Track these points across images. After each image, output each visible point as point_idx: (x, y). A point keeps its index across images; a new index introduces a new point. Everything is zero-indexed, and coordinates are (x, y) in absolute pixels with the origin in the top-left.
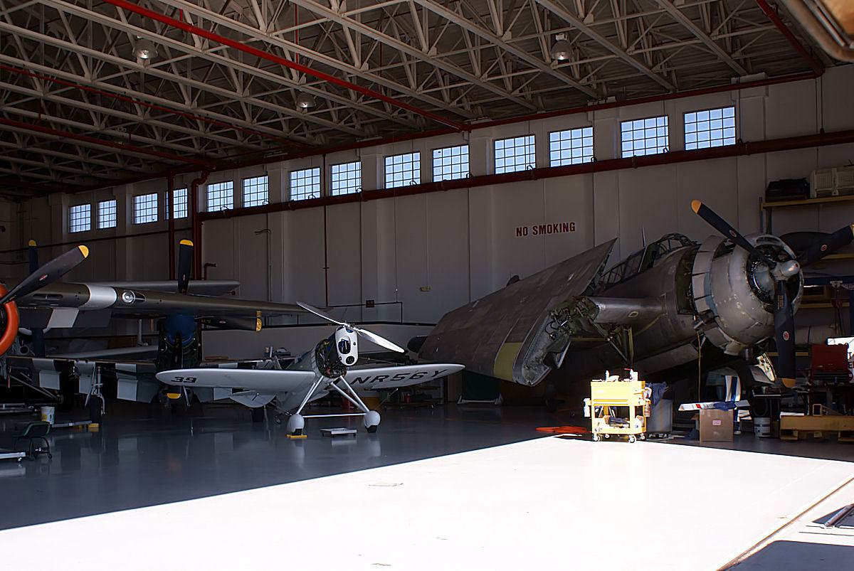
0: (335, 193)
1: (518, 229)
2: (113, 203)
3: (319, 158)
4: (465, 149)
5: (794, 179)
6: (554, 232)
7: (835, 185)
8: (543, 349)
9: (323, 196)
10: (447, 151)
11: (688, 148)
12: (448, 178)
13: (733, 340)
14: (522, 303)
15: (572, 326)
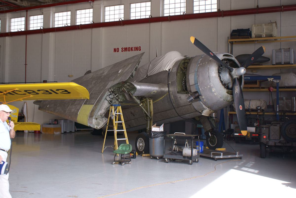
0: (31, 29)
1: (114, 49)
3: (24, 13)
4: (91, 10)
5: (244, 29)
6: (131, 51)
7: (263, 32)
10: (83, 11)
11: (195, 12)
13: (208, 108)
14: (94, 84)
15: (120, 97)
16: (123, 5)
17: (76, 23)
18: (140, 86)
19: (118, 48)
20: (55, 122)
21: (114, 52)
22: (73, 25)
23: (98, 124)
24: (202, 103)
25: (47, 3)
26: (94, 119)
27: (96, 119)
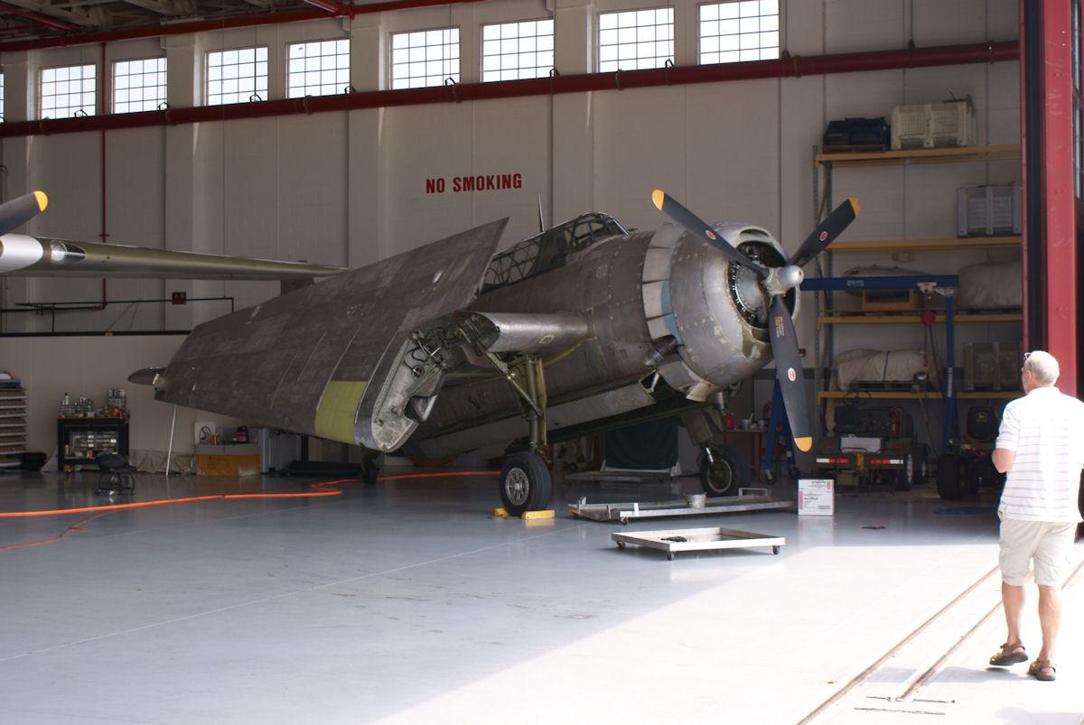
1: (428, 181)
3: (93, 49)
4: (344, 45)
6: (488, 188)
7: (928, 131)
8: (402, 392)
10: (313, 48)
12: (315, 92)
13: (702, 380)
16: (457, 30)
18: (509, 323)
19: (443, 180)
20: (238, 436)
21: (428, 192)
22: (279, 97)
23: (388, 438)
24: (686, 367)
25: (179, 17)
26: (375, 422)
27: (382, 422)
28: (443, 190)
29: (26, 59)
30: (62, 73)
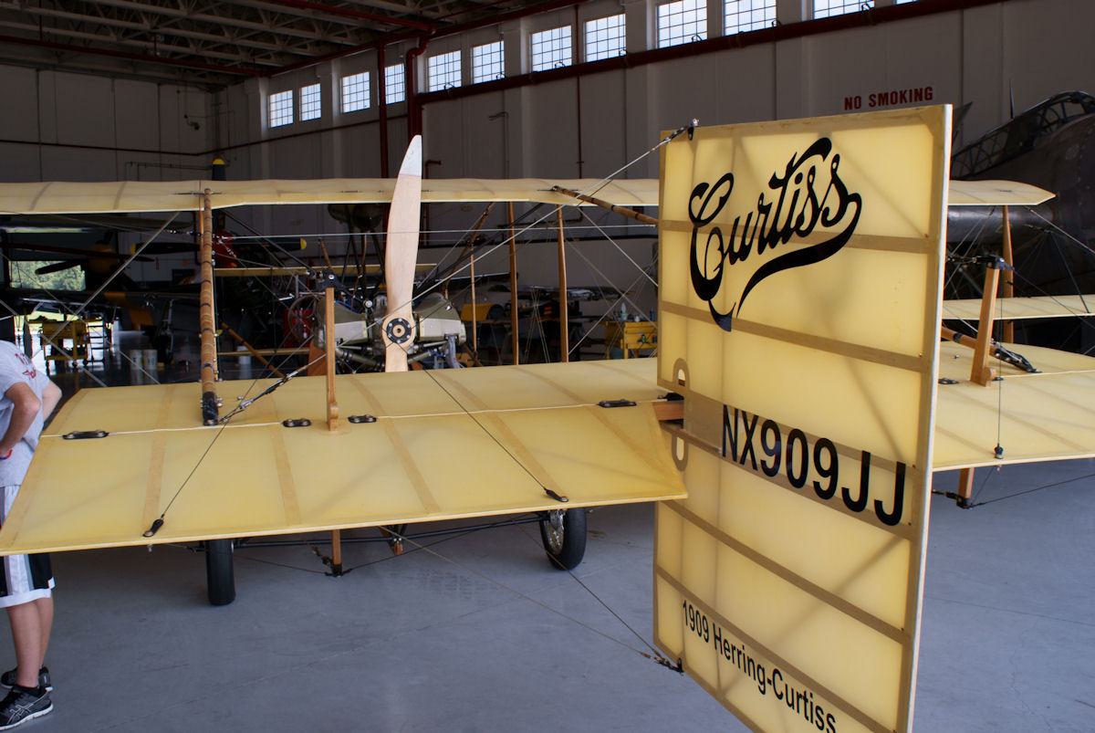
0: (591, 59)
1: (846, 99)
2: (318, 87)
3: (568, 12)
9: (575, 63)
12: (746, 29)
17: (725, 28)
21: (846, 109)
22: (716, 35)
28: (860, 105)
29: (519, 26)
30: (547, 34)
